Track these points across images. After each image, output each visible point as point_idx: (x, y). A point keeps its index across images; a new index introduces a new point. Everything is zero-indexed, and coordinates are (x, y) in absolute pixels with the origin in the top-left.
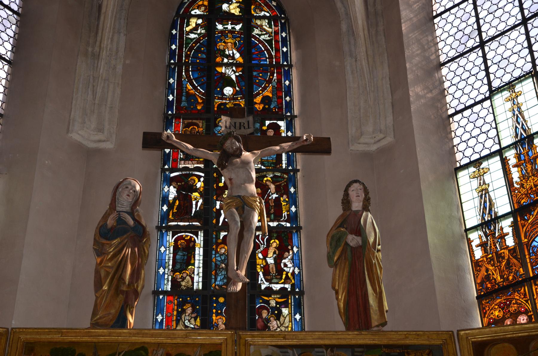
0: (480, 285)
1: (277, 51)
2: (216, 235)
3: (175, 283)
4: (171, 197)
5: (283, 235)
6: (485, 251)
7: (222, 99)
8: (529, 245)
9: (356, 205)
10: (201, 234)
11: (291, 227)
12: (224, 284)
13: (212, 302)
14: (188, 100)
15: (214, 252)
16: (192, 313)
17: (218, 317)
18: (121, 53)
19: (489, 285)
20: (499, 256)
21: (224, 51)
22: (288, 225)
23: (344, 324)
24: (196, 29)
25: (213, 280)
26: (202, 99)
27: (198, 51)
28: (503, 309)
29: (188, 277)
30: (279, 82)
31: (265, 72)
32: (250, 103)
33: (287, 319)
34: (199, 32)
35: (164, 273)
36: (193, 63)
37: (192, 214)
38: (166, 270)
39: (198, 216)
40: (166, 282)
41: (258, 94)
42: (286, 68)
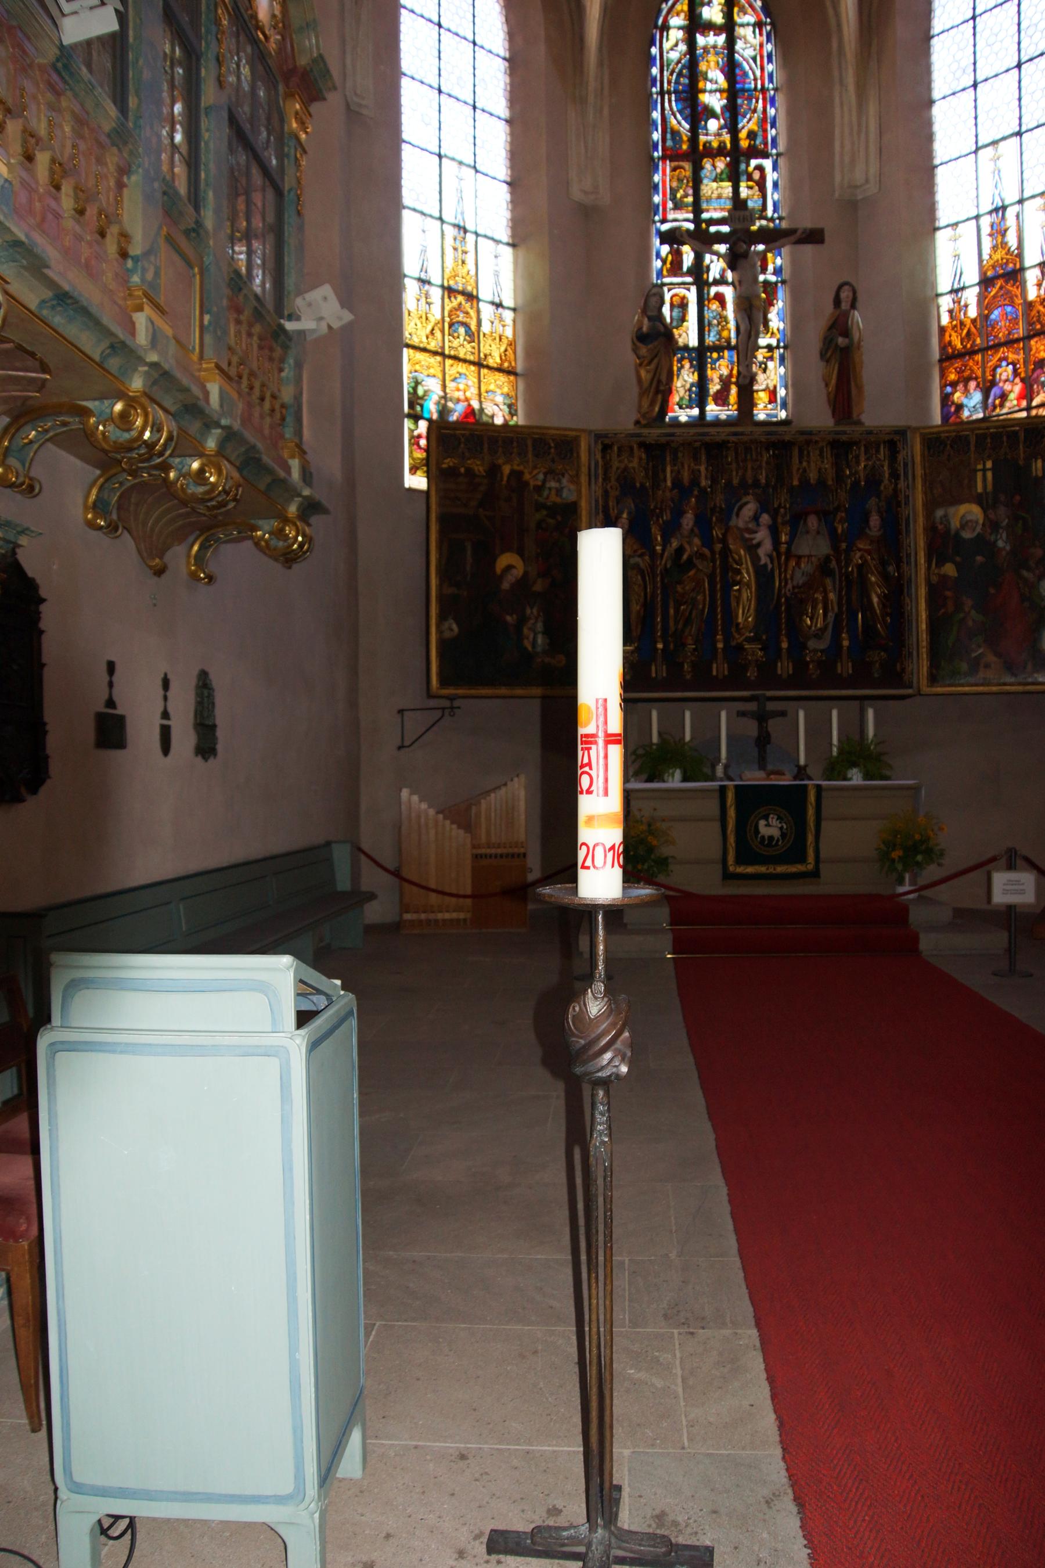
0: (943, 348)
1: (762, 69)
6: (951, 317)
7: (707, 135)
8: (987, 317)
9: (845, 306)
10: (694, 289)
12: (719, 340)
13: (707, 358)
14: (673, 139)
15: (706, 308)
16: (690, 368)
18: (606, 92)
19: (950, 351)
20: (962, 324)
21: (706, 73)
22: (773, 278)
24: (676, 45)
25: (707, 336)
26: (686, 135)
27: (680, 74)
28: (958, 373)
31: (749, 99)
32: (735, 140)
33: (773, 373)
36: (676, 92)
39: (689, 273)
41: (743, 127)
42: (772, 93)
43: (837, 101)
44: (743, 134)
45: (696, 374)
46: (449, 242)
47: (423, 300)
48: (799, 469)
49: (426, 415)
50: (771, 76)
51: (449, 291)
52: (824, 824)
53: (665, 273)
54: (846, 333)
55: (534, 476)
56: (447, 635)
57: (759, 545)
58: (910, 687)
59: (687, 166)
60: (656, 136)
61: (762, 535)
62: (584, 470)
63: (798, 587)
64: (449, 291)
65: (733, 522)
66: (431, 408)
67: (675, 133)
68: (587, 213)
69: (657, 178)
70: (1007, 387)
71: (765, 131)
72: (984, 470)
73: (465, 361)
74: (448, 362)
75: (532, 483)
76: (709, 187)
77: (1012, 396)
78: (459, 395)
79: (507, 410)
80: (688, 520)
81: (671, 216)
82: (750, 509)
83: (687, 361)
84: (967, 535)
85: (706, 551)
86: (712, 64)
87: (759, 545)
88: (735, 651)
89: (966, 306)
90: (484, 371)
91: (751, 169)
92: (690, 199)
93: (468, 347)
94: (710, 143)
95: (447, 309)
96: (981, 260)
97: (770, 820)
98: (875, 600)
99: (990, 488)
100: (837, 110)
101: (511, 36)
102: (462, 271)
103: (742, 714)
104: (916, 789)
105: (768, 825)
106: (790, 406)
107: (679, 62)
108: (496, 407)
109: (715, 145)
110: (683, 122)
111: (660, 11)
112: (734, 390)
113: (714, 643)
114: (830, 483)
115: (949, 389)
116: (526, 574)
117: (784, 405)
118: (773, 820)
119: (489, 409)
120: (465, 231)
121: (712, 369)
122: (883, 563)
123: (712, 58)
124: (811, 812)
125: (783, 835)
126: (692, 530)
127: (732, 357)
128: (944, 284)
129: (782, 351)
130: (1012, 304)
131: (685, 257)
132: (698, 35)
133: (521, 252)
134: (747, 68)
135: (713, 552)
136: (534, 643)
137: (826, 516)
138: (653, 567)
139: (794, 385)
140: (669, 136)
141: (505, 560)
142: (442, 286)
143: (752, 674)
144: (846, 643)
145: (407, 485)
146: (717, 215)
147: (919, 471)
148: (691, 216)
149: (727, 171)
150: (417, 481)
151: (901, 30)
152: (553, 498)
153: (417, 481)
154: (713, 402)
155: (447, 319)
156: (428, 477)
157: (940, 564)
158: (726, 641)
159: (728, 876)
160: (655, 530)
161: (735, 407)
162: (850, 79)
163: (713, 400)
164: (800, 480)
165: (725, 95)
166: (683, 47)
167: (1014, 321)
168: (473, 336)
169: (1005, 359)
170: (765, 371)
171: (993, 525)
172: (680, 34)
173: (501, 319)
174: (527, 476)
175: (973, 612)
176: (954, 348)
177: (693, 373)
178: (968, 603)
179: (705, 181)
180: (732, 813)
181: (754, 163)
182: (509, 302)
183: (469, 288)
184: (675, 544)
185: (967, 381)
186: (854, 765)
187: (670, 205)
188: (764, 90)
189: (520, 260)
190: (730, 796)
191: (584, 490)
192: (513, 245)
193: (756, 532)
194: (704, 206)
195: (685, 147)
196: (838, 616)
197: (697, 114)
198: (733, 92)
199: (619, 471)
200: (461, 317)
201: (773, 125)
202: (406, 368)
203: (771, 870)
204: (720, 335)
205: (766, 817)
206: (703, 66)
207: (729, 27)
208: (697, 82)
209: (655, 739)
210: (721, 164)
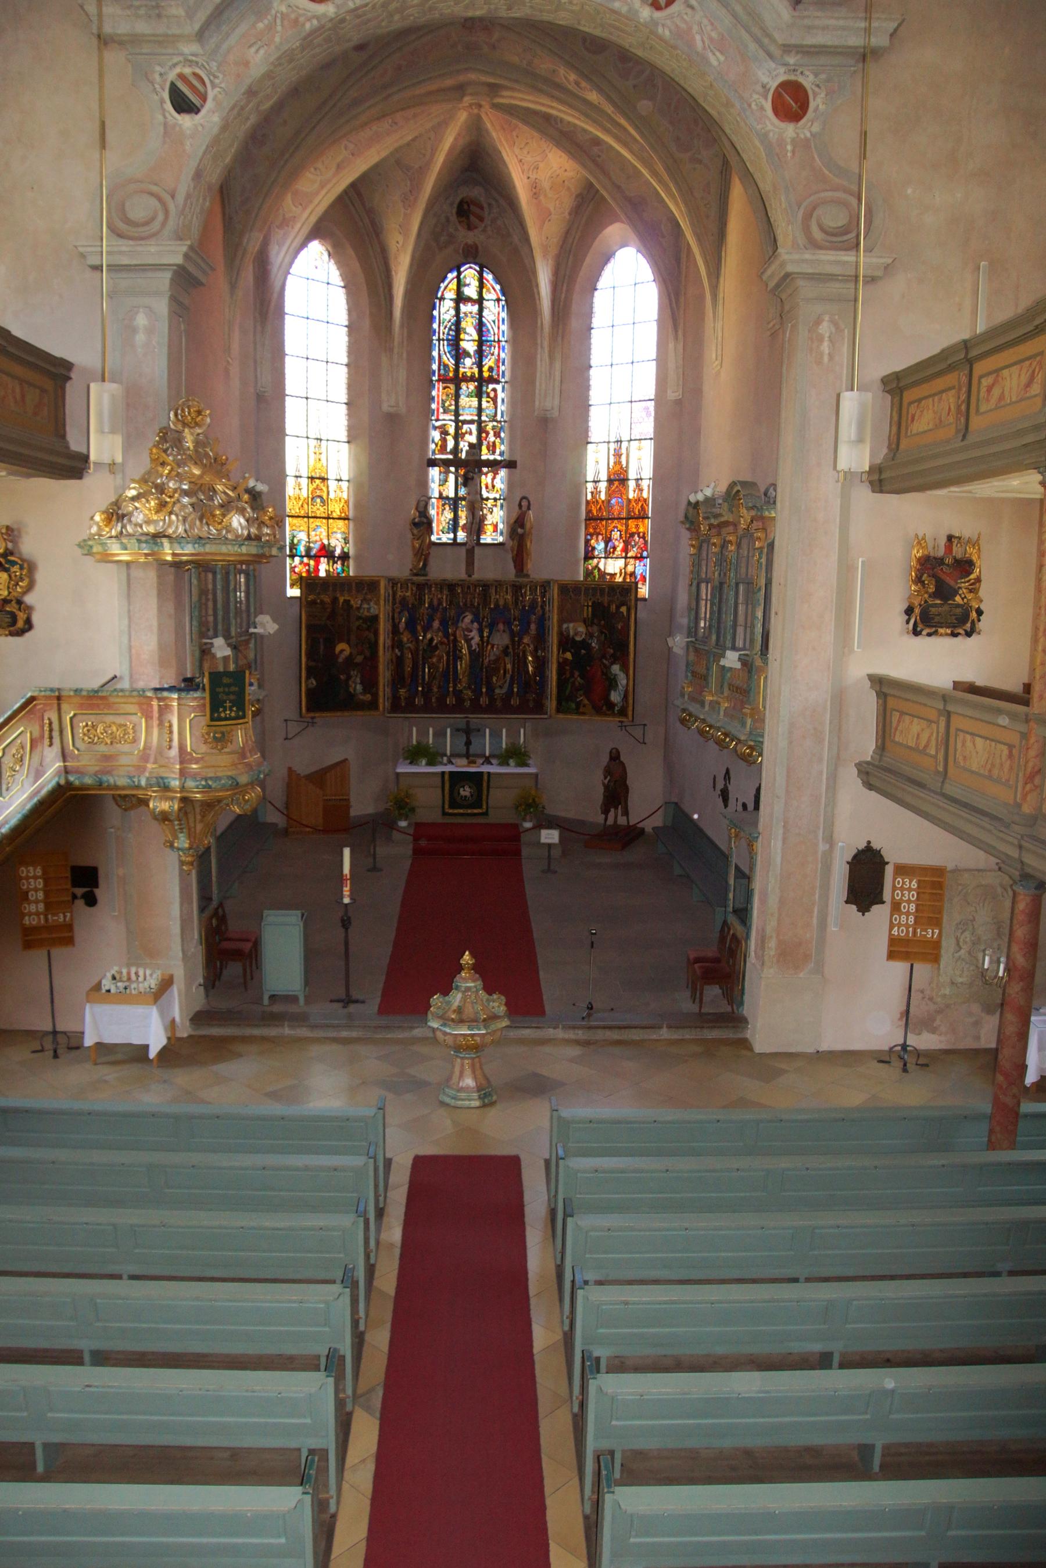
0: (589, 512)
1: (499, 328)
3: (441, 494)
4: (436, 440)
8: (609, 501)
9: (524, 508)
14: (444, 369)
18: (405, 343)
27: (450, 329)
30: (499, 355)
31: (490, 346)
32: (481, 372)
34: (450, 312)
36: (448, 340)
39: (451, 453)
43: (539, 356)
44: (485, 369)
46: (312, 450)
47: (297, 488)
49: (299, 554)
50: (503, 332)
51: (312, 479)
53: (437, 452)
54: (522, 526)
55: (355, 603)
56: (310, 686)
57: (472, 638)
58: (546, 714)
59: (452, 386)
60: (435, 367)
61: (474, 634)
62: (382, 597)
64: (312, 479)
65: (460, 624)
66: (302, 549)
67: (446, 366)
68: (392, 419)
69: (434, 393)
70: (617, 543)
71: (498, 367)
72: (588, 606)
73: (320, 518)
74: (311, 520)
75: (355, 606)
76: (464, 401)
77: (619, 549)
78: (318, 538)
80: (436, 624)
81: (441, 417)
82: (469, 618)
84: (578, 639)
85: (445, 640)
86: (469, 324)
87: (472, 638)
88: (458, 694)
89: (600, 492)
90: (331, 521)
91: (489, 390)
92: (453, 407)
93: (322, 509)
94: (465, 373)
95: (310, 489)
96: (609, 468)
98: (530, 669)
99: (590, 616)
100: (539, 363)
101: (350, 311)
102: (319, 465)
103: (458, 730)
104: (536, 775)
107: (450, 321)
109: (469, 374)
110: (451, 359)
111: (439, 287)
113: (448, 688)
115: (589, 537)
116: (351, 653)
117: (502, 534)
118: (467, 789)
119: (333, 542)
120: (321, 440)
122: (536, 650)
123: (469, 319)
124: (485, 785)
125: (472, 796)
128: (590, 478)
130: (621, 498)
131: (448, 442)
132: (461, 305)
133: (353, 446)
134: (490, 328)
135: (449, 641)
136: (355, 689)
137: (508, 623)
138: (417, 649)
140: (442, 367)
141: (341, 646)
142: (308, 478)
143: (467, 704)
144: (515, 690)
145: (288, 595)
146: (468, 418)
147: (556, 604)
148: (453, 418)
149: (475, 391)
150: (294, 592)
151: (574, 324)
152: (366, 613)
153: (294, 592)
155: (310, 496)
156: (301, 589)
157: (564, 652)
159: (444, 814)
160: (419, 628)
162: (546, 344)
165: (476, 343)
166: (453, 312)
167: (622, 507)
168: (324, 502)
169: (617, 527)
170: (491, 513)
171: (591, 635)
172: (452, 304)
173: (341, 488)
174: (352, 602)
175: (579, 679)
176: (593, 514)
178: (577, 674)
179: (462, 397)
181: (491, 386)
182: (345, 476)
183: (323, 475)
184: (429, 636)
185: (598, 534)
186: (511, 757)
187: (441, 410)
188: (499, 341)
190: (447, 777)
191: (382, 609)
192: (348, 442)
193: (471, 631)
194: (461, 412)
195: (451, 375)
196: (512, 677)
197: (459, 355)
198: (481, 343)
200: (318, 493)
201: (503, 364)
202: (288, 528)
205: (463, 787)
206: (463, 324)
207: (480, 301)
208: (460, 334)
209: (414, 742)
210: (472, 386)
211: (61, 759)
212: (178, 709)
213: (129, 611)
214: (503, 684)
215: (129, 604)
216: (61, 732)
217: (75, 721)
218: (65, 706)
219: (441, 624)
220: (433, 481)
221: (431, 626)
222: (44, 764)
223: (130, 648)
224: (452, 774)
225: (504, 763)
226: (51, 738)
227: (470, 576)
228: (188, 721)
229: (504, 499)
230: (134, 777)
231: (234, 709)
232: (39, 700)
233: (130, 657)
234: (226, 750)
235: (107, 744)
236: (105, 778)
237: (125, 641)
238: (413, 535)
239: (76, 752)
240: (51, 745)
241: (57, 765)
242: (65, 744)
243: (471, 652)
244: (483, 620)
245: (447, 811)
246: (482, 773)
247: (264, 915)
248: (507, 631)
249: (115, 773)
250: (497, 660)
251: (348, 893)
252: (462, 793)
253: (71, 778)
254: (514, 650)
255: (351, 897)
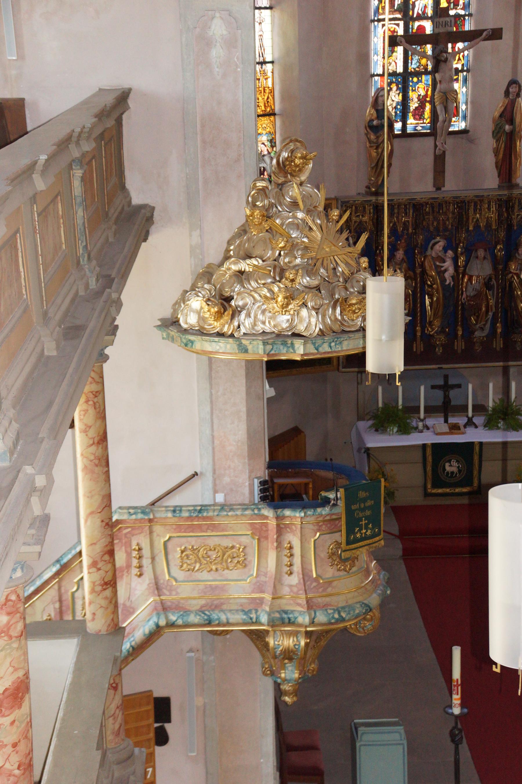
2: (412, 26)
5: (458, 22)
10: (401, 23)
11: (465, 15)
12: (418, 67)
16: (397, 90)
17: (414, 93)
22: (462, 12)
23: (497, 163)
25: (410, 64)
29: (393, 63)
35: (377, 60)
37: (394, 6)
38: (379, 56)
40: (379, 66)
45: (401, 94)
48: (473, 218)
52: (483, 463)
54: (511, 121)
61: (448, 264)
63: (470, 296)
65: (429, 252)
79: (268, 144)
83: (395, 84)
87: (446, 270)
97: (452, 463)
103: (433, 387)
105: (451, 466)
106: (468, 118)
108: (263, 145)
112: (428, 107)
114: (494, 227)
117: (465, 118)
118: (454, 463)
121: (413, 91)
124: (476, 458)
125: (460, 471)
126: (403, 259)
127: (427, 81)
129: (465, 73)
137: (491, 249)
139: (472, 103)
143: (439, 351)
144: (499, 330)
154: (412, 117)
158: (423, 328)
159: (427, 495)
161: (428, 120)
163: (412, 116)
164: (474, 227)
177: (399, 94)
180: (430, 459)
189: (276, 21)
199: (356, 224)
203: (452, 491)
204: (420, 63)
205: (450, 461)
209: (380, 405)
211: (156, 592)
212: (301, 528)
213: (211, 393)
214: (485, 325)
215: (211, 384)
216: (153, 559)
217: (170, 545)
218: (157, 529)
219: (406, 253)
220: (376, 53)
221: (394, 255)
222: (133, 599)
223: (213, 437)
224: (435, 446)
225: (490, 424)
226: (140, 567)
227: (438, 189)
228: (313, 540)
229: (468, 71)
230: (250, 611)
231: (370, 526)
232: (128, 523)
233: (213, 449)
234: (354, 569)
235: (211, 570)
236: (214, 616)
237: (208, 432)
238: (370, 141)
239: (174, 583)
240: (141, 575)
241: (152, 599)
242: (158, 572)
243: (445, 288)
244: (459, 244)
245: (429, 491)
246: (472, 443)
247: (360, 733)
248: (489, 257)
249: (224, 607)
250: (478, 295)
251: (459, 702)
252: (448, 468)
253: (173, 618)
254: (497, 282)
255: (463, 705)
